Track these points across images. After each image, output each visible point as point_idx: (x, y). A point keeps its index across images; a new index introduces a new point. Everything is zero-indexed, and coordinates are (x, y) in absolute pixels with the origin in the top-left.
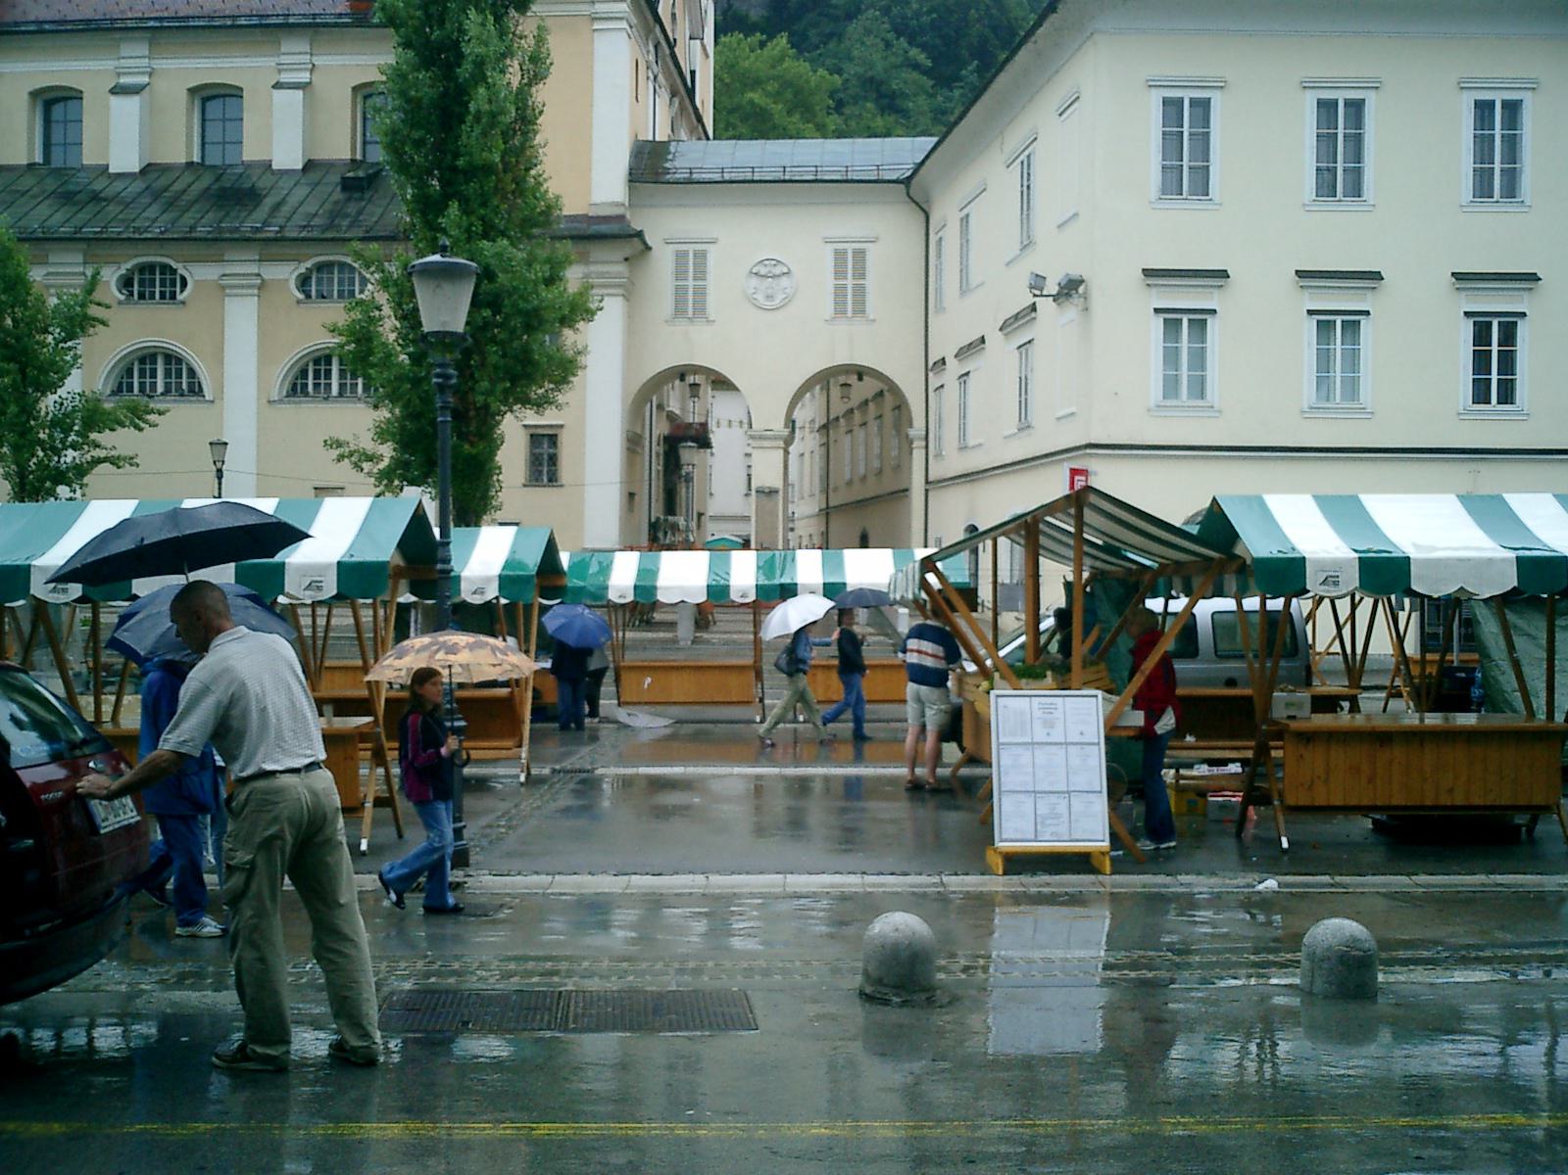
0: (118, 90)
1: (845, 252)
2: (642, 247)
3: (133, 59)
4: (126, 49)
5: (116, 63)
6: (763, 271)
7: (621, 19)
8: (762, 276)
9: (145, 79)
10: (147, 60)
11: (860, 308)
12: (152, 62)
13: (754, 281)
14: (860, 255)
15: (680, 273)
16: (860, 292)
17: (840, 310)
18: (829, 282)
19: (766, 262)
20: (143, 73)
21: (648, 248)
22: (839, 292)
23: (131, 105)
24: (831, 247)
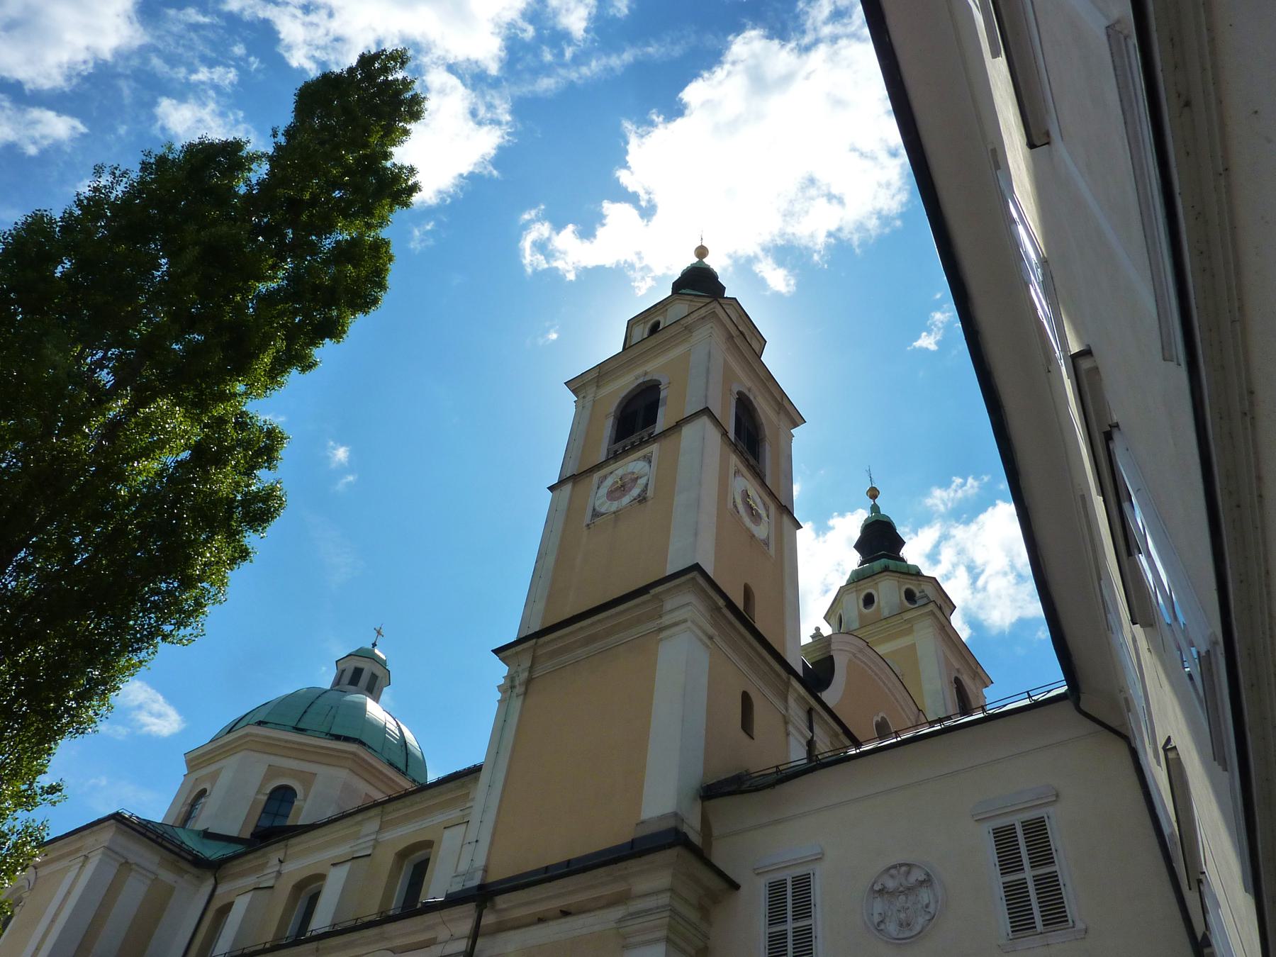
1: (1011, 829)
2: (715, 883)
6: (891, 884)
7: (685, 621)
8: (891, 893)
11: (1056, 915)
13: (879, 906)
14: (1037, 830)
15: (776, 915)
16: (1050, 887)
17: (1021, 921)
18: (995, 882)
19: (893, 872)
21: (735, 886)
22: (1015, 895)
24: (988, 827)
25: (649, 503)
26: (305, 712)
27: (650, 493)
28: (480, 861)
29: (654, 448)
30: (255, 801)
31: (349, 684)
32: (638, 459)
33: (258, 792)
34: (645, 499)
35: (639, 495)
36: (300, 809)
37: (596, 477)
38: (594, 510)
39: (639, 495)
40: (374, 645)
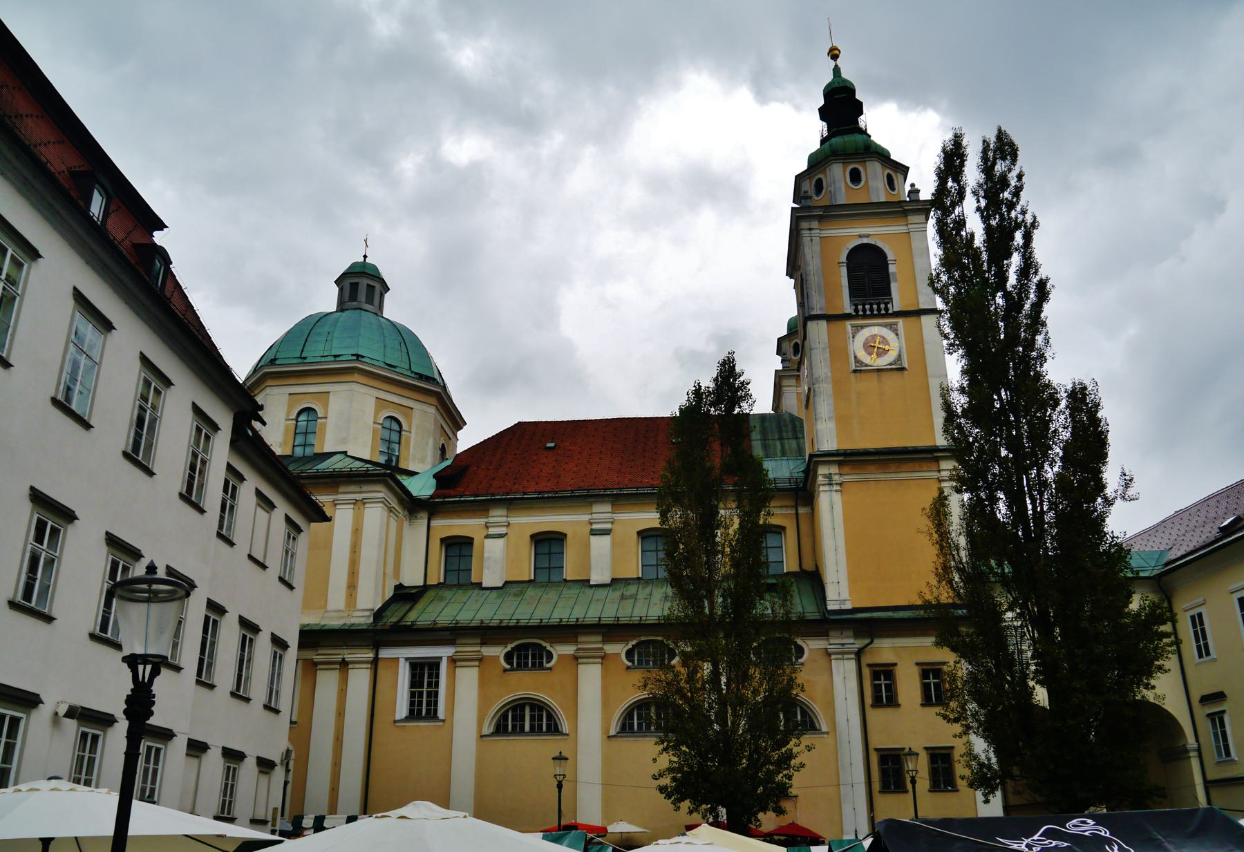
0: (594, 533)
3: (602, 512)
4: (596, 508)
5: (590, 517)
9: (608, 526)
10: (610, 515)
12: (614, 515)
20: (610, 522)
23: (606, 540)
25: (905, 372)
26: (385, 346)
27: (906, 366)
28: (845, 595)
29: (900, 322)
30: (375, 432)
31: (366, 303)
32: (886, 326)
33: (375, 423)
34: (903, 369)
35: (895, 363)
36: (408, 439)
37: (848, 324)
38: (855, 357)
39: (894, 361)
40: (365, 257)
